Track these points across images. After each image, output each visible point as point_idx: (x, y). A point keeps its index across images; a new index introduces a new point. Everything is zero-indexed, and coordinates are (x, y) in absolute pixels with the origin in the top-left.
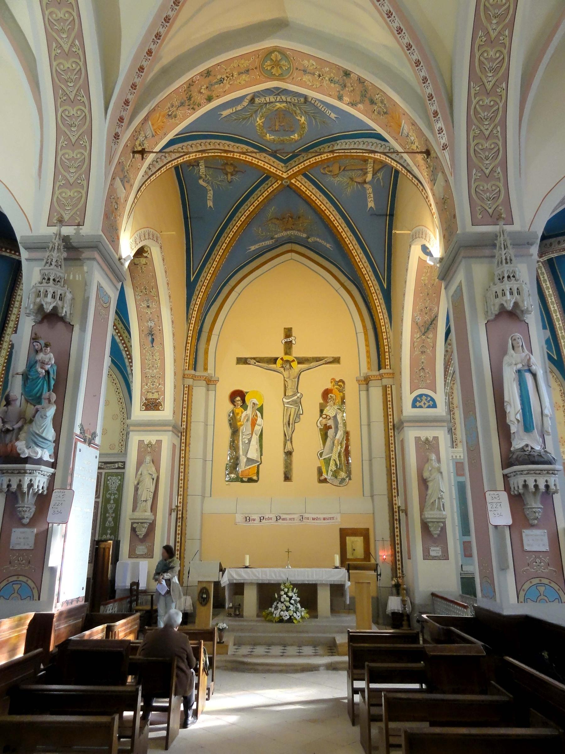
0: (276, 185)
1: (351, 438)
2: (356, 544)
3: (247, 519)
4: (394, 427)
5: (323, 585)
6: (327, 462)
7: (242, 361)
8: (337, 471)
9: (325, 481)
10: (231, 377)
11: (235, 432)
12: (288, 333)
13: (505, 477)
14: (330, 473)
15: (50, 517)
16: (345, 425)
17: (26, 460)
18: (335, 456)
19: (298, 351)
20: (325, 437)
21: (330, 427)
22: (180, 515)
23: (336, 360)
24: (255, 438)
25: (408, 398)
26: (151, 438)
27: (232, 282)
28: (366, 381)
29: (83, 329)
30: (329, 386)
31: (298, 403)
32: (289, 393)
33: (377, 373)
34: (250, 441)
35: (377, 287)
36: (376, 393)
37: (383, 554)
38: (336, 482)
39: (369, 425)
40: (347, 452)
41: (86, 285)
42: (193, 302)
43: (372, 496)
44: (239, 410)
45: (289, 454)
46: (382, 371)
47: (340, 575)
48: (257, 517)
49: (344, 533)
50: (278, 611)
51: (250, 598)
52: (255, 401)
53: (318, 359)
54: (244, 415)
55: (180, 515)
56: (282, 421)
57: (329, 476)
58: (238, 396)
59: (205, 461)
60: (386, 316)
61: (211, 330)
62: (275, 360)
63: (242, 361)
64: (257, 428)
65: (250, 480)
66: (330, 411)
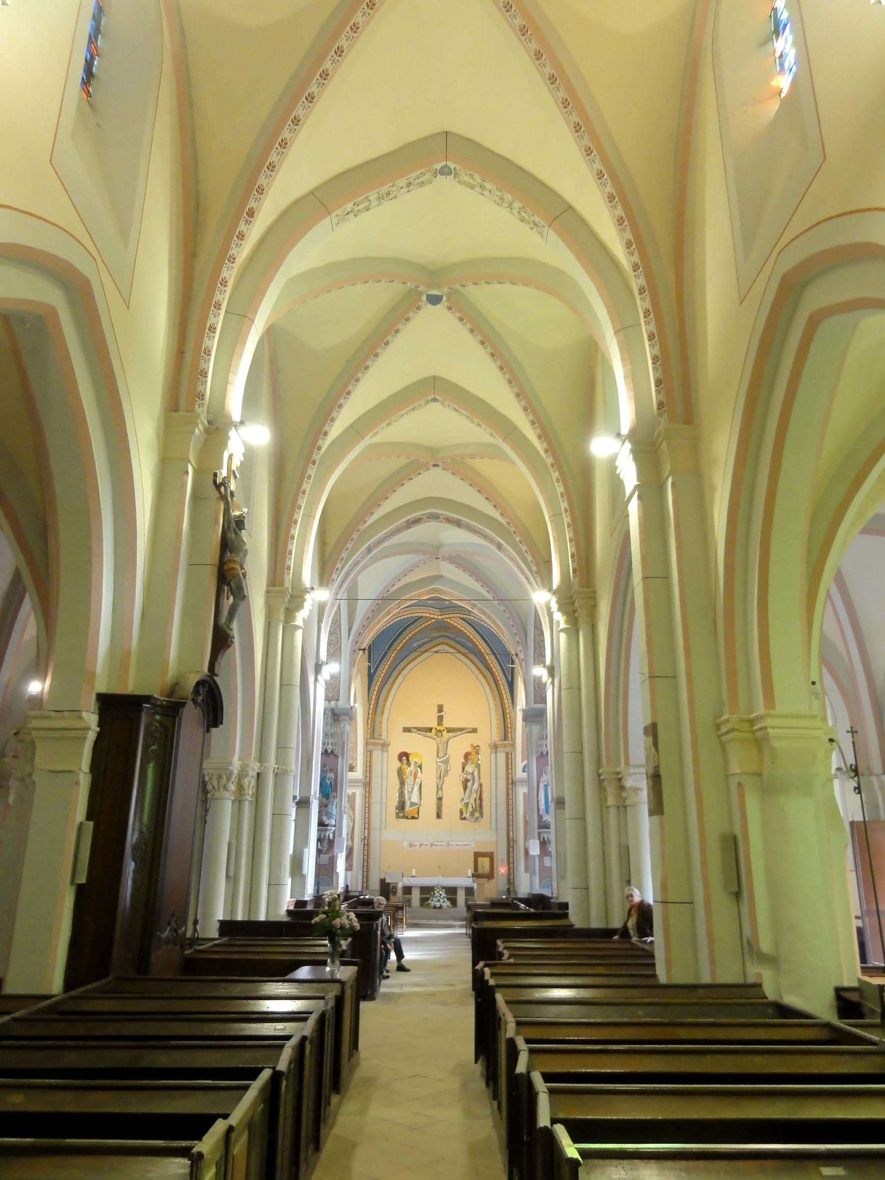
0: (433, 621)
1: (484, 788)
2: (484, 862)
3: (411, 845)
4: (511, 783)
5: (461, 887)
6: (467, 805)
7: (407, 730)
8: (476, 810)
9: (465, 819)
10: (399, 742)
11: (402, 783)
12: (440, 709)
13: (539, 834)
14: (468, 813)
15: (335, 850)
16: (479, 778)
17: (327, 826)
18: (472, 801)
19: (447, 724)
20: (465, 788)
21: (469, 780)
22: (366, 842)
23: (474, 731)
24: (416, 788)
25: (520, 764)
26: (350, 791)
27: (399, 668)
28: (495, 747)
29: (343, 758)
30: (469, 750)
31: (446, 762)
32: (441, 755)
33: (502, 743)
34: (413, 789)
35: (504, 680)
36: (502, 757)
37: (503, 870)
38: (473, 820)
39: (496, 779)
40: (481, 799)
41: (343, 734)
42: (372, 688)
43: (497, 830)
44: (405, 767)
45: (440, 799)
46: (506, 742)
47: (469, 882)
48: (417, 844)
49: (477, 855)
50: (433, 902)
51: (416, 896)
52: (416, 760)
53: (461, 729)
54: (408, 770)
55: (366, 842)
56: (435, 776)
57: (467, 815)
58: (404, 756)
59: (381, 803)
60: (510, 701)
61: (384, 706)
62: (430, 730)
63: (407, 730)
64: (418, 780)
65: (413, 818)
66: (470, 768)
